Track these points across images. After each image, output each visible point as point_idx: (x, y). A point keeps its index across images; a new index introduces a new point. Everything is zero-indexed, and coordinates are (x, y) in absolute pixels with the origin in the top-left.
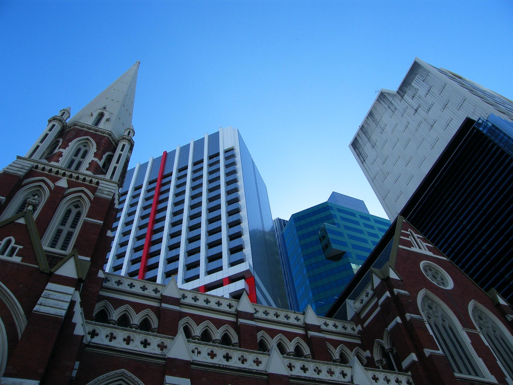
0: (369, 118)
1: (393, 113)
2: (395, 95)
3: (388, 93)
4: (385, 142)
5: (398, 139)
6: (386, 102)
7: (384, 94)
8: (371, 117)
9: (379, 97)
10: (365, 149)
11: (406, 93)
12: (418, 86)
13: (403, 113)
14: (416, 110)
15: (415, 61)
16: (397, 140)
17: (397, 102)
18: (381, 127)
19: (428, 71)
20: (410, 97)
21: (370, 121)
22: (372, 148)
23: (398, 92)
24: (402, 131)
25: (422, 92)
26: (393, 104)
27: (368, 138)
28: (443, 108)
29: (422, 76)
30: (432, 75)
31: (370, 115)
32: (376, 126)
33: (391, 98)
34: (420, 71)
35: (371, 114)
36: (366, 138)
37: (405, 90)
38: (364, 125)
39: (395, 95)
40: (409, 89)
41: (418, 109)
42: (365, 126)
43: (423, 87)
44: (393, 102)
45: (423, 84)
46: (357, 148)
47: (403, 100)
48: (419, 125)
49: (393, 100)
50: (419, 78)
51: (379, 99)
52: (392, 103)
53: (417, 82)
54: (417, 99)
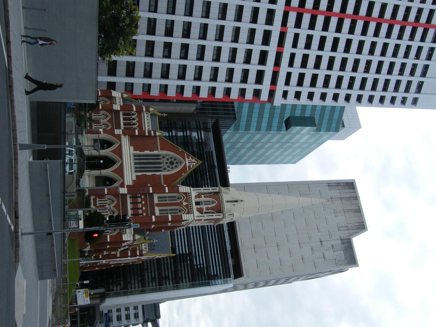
0: (357, 208)
1: (339, 227)
2: (350, 236)
3: (358, 232)
4: (324, 209)
5: (317, 219)
6: (353, 227)
7: (361, 230)
8: (356, 210)
9: (364, 224)
10: (338, 191)
11: (342, 243)
12: (336, 254)
13: (330, 233)
14: (321, 242)
15: (356, 264)
16: (316, 218)
17: (344, 234)
18: (339, 212)
19: (338, 266)
20: (334, 244)
21: (354, 207)
22: (332, 197)
23: (350, 239)
24: (319, 225)
25: (330, 254)
26: (345, 230)
27: (343, 198)
28: (303, 257)
29: (340, 260)
30: (332, 266)
31: (359, 210)
32: (344, 209)
33: (352, 232)
34: (344, 262)
35: (359, 210)
36: (344, 196)
37: (345, 244)
38: (356, 201)
39: (350, 236)
40: (342, 248)
41: (321, 243)
42: (354, 202)
43: (331, 256)
44: (348, 232)
45: (333, 257)
46: (345, 185)
47: (340, 239)
48: (310, 238)
49: (348, 232)
50: (341, 258)
51: (363, 224)
52: (347, 230)
53: (340, 255)
54: (328, 248)
